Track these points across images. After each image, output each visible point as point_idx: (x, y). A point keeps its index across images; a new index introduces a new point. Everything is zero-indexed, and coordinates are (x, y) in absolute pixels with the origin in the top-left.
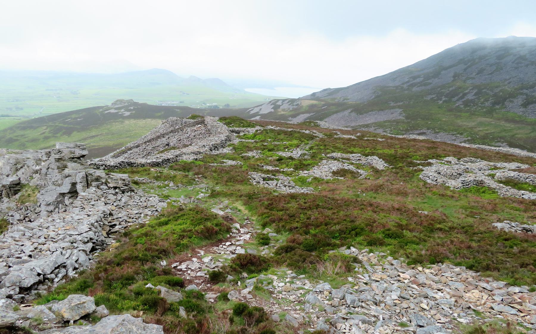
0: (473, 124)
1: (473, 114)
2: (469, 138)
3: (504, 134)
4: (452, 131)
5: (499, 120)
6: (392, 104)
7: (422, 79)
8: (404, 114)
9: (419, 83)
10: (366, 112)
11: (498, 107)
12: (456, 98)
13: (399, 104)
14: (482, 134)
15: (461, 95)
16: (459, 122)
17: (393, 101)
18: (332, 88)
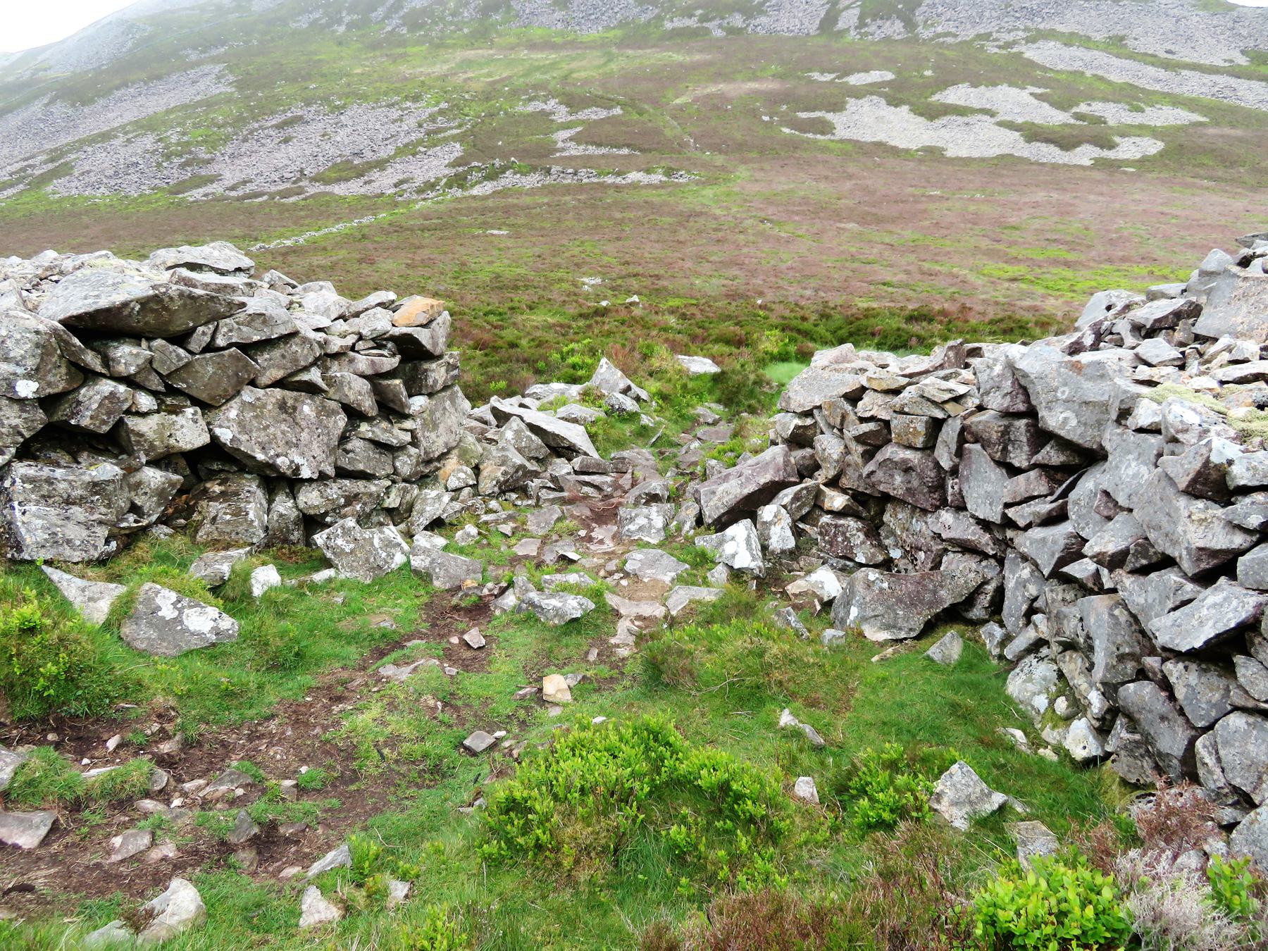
0: (446, 67)
1: (438, 46)
2: (444, 105)
3: (538, 77)
4: (386, 94)
5: (512, 49)
6: (193, 57)
8: (231, 78)
10: (106, 93)
11: (497, 17)
12: (381, 11)
13: (214, 52)
14: (476, 86)
16: (405, 69)
17: (195, 48)
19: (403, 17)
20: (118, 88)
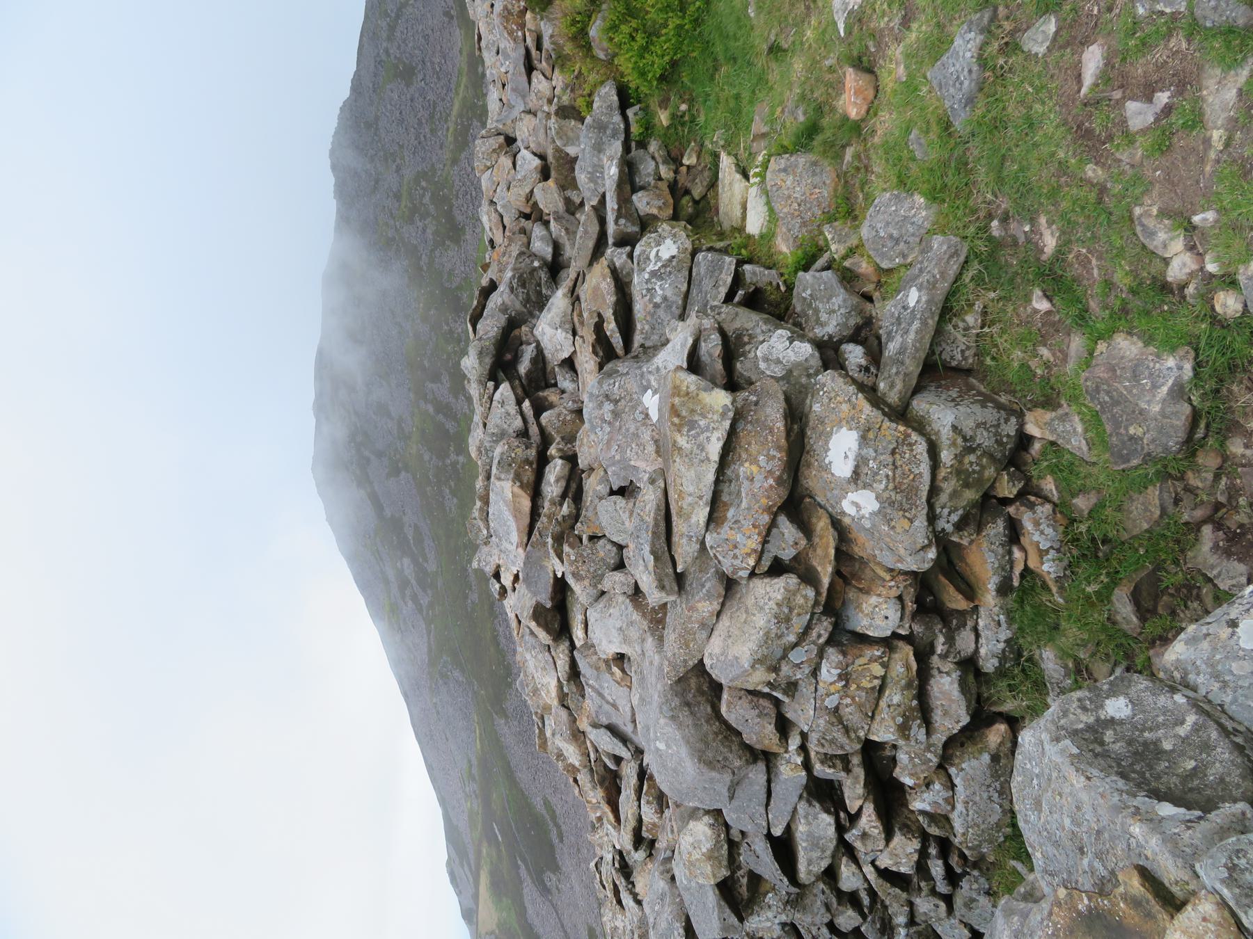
7: (406, 561)
9: (415, 562)
15: (440, 417)
17: (466, 597)
18: (445, 857)
19: (457, 399)
20: (498, 645)
